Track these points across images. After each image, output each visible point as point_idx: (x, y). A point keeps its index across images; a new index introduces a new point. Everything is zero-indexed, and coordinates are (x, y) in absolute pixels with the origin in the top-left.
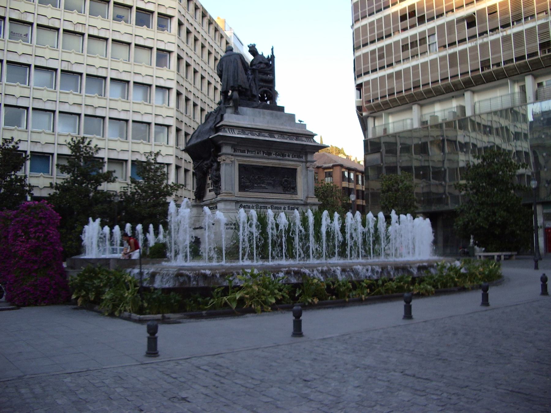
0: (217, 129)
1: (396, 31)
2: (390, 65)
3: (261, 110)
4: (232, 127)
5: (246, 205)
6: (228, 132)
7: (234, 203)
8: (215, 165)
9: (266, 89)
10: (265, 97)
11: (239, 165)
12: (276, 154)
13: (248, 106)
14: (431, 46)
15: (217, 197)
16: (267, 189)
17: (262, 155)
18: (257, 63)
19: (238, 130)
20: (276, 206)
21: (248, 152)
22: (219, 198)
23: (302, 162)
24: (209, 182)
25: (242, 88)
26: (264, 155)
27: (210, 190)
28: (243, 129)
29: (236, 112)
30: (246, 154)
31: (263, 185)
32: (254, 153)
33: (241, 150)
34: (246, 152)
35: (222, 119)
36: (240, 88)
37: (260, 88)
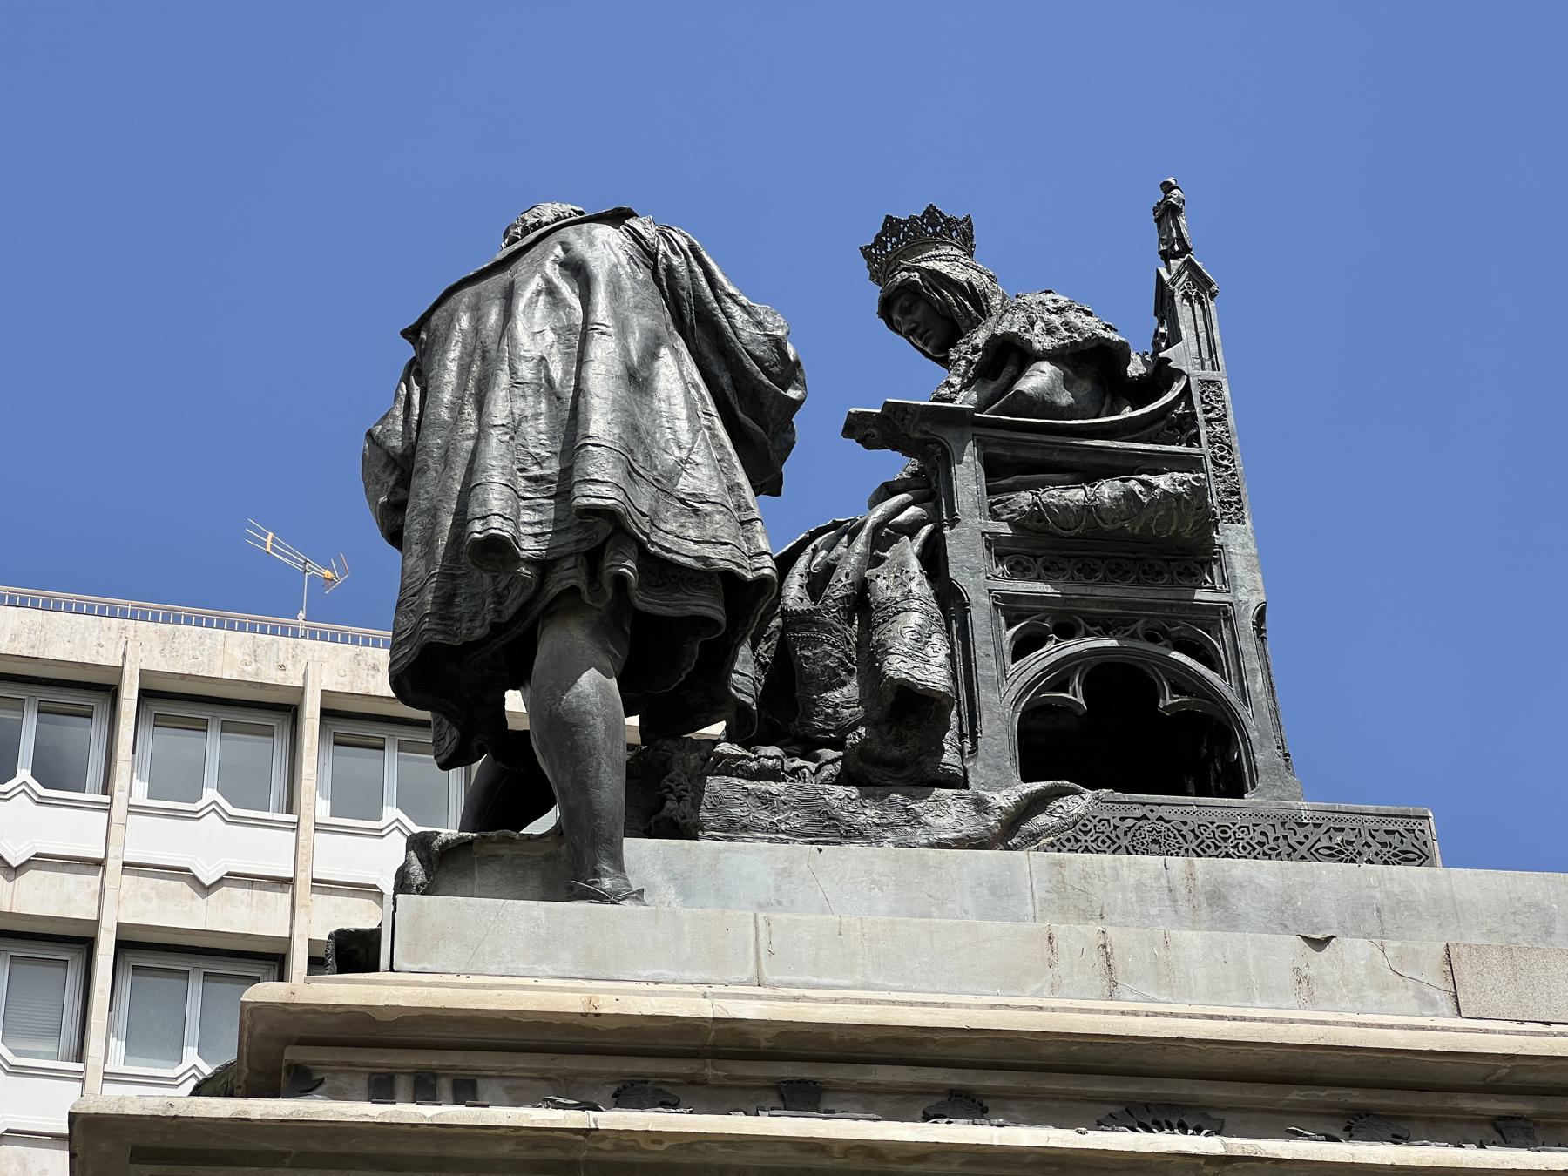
25: (661, 570)
37: (1023, 647)
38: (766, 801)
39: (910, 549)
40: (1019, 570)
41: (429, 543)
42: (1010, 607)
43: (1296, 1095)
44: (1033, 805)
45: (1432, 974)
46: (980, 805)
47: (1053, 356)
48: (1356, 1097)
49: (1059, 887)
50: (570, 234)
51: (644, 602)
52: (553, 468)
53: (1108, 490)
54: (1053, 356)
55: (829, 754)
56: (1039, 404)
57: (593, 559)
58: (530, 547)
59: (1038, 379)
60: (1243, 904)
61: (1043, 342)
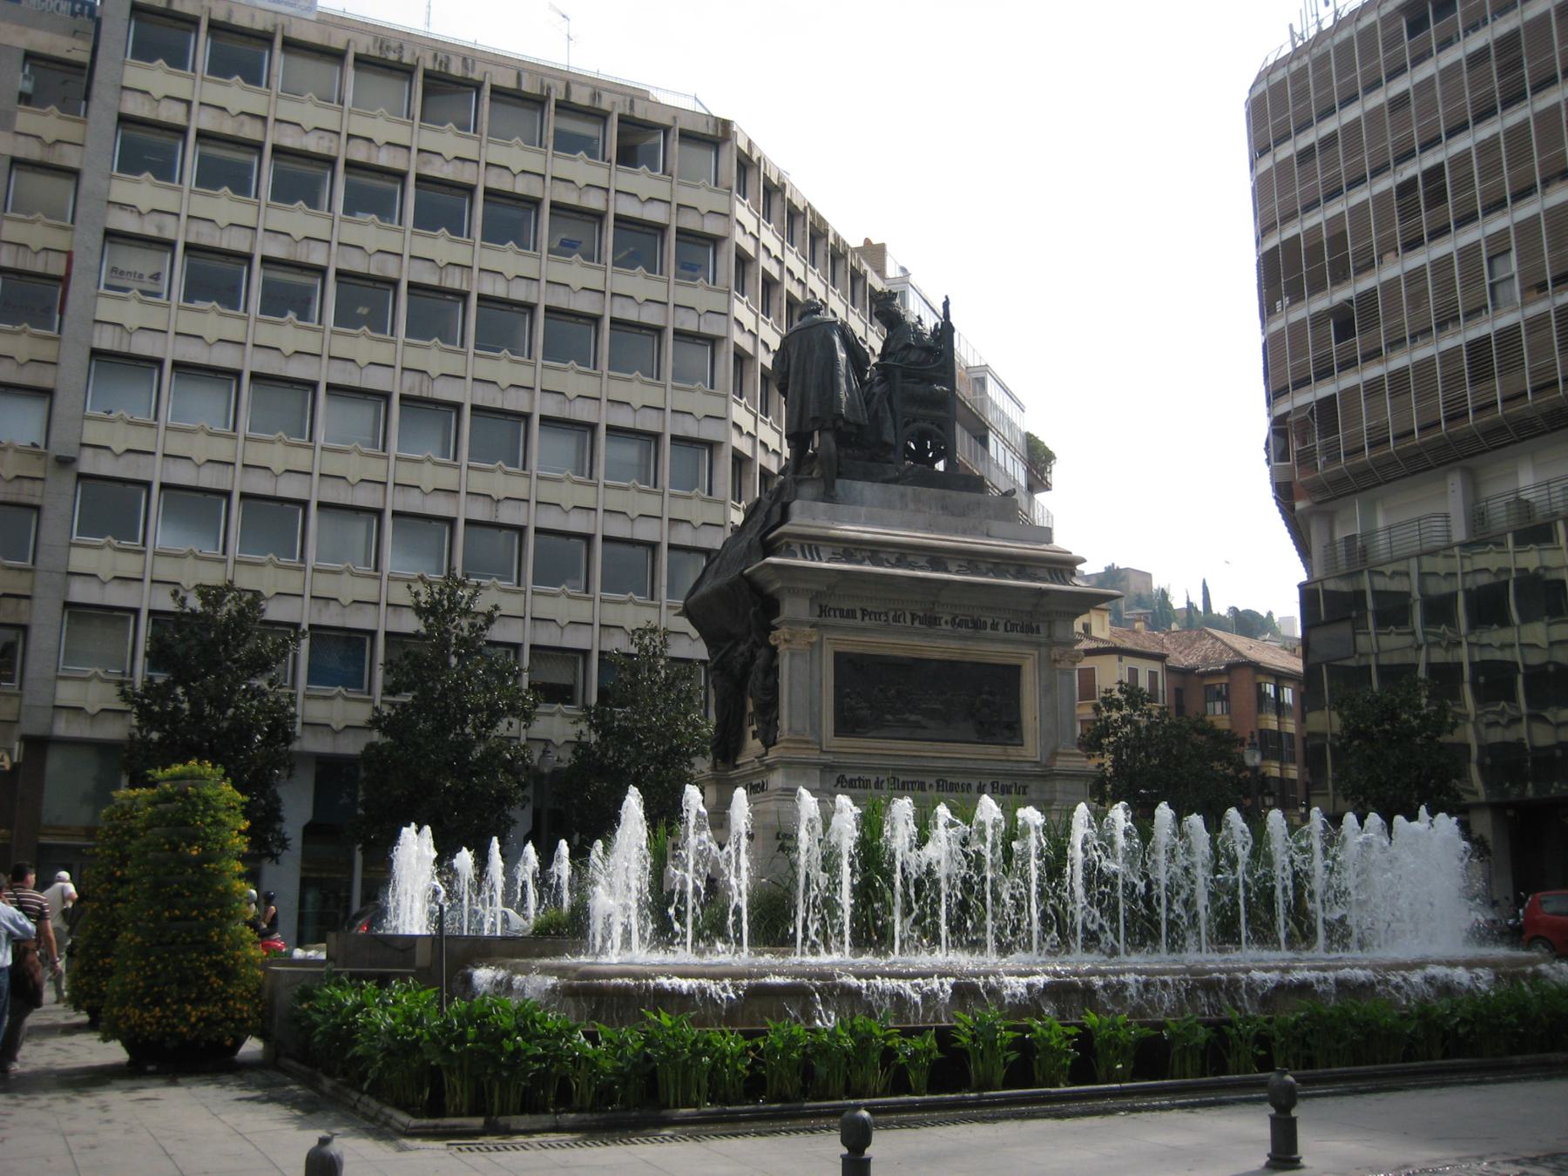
0: (769, 549)
1: (1387, 247)
2: (1373, 355)
3: (909, 490)
4: (813, 544)
5: (856, 776)
6: (799, 555)
7: (818, 772)
8: (762, 654)
9: (926, 425)
10: (929, 451)
11: (839, 657)
12: (954, 620)
13: (868, 476)
14: (1500, 291)
15: (766, 754)
16: (925, 728)
17: (909, 623)
18: (900, 346)
19: (830, 550)
20: (955, 781)
21: (863, 616)
22: (773, 754)
23: (1038, 645)
24: (750, 708)
26: (917, 624)
27: (754, 732)
28: (851, 548)
29: (829, 496)
30: (858, 622)
31: (913, 718)
32: (883, 618)
33: (841, 610)
34: (859, 614)
35: (785, 517)
36: (841, 423)
37: (906, 425)
46: (898, 470)
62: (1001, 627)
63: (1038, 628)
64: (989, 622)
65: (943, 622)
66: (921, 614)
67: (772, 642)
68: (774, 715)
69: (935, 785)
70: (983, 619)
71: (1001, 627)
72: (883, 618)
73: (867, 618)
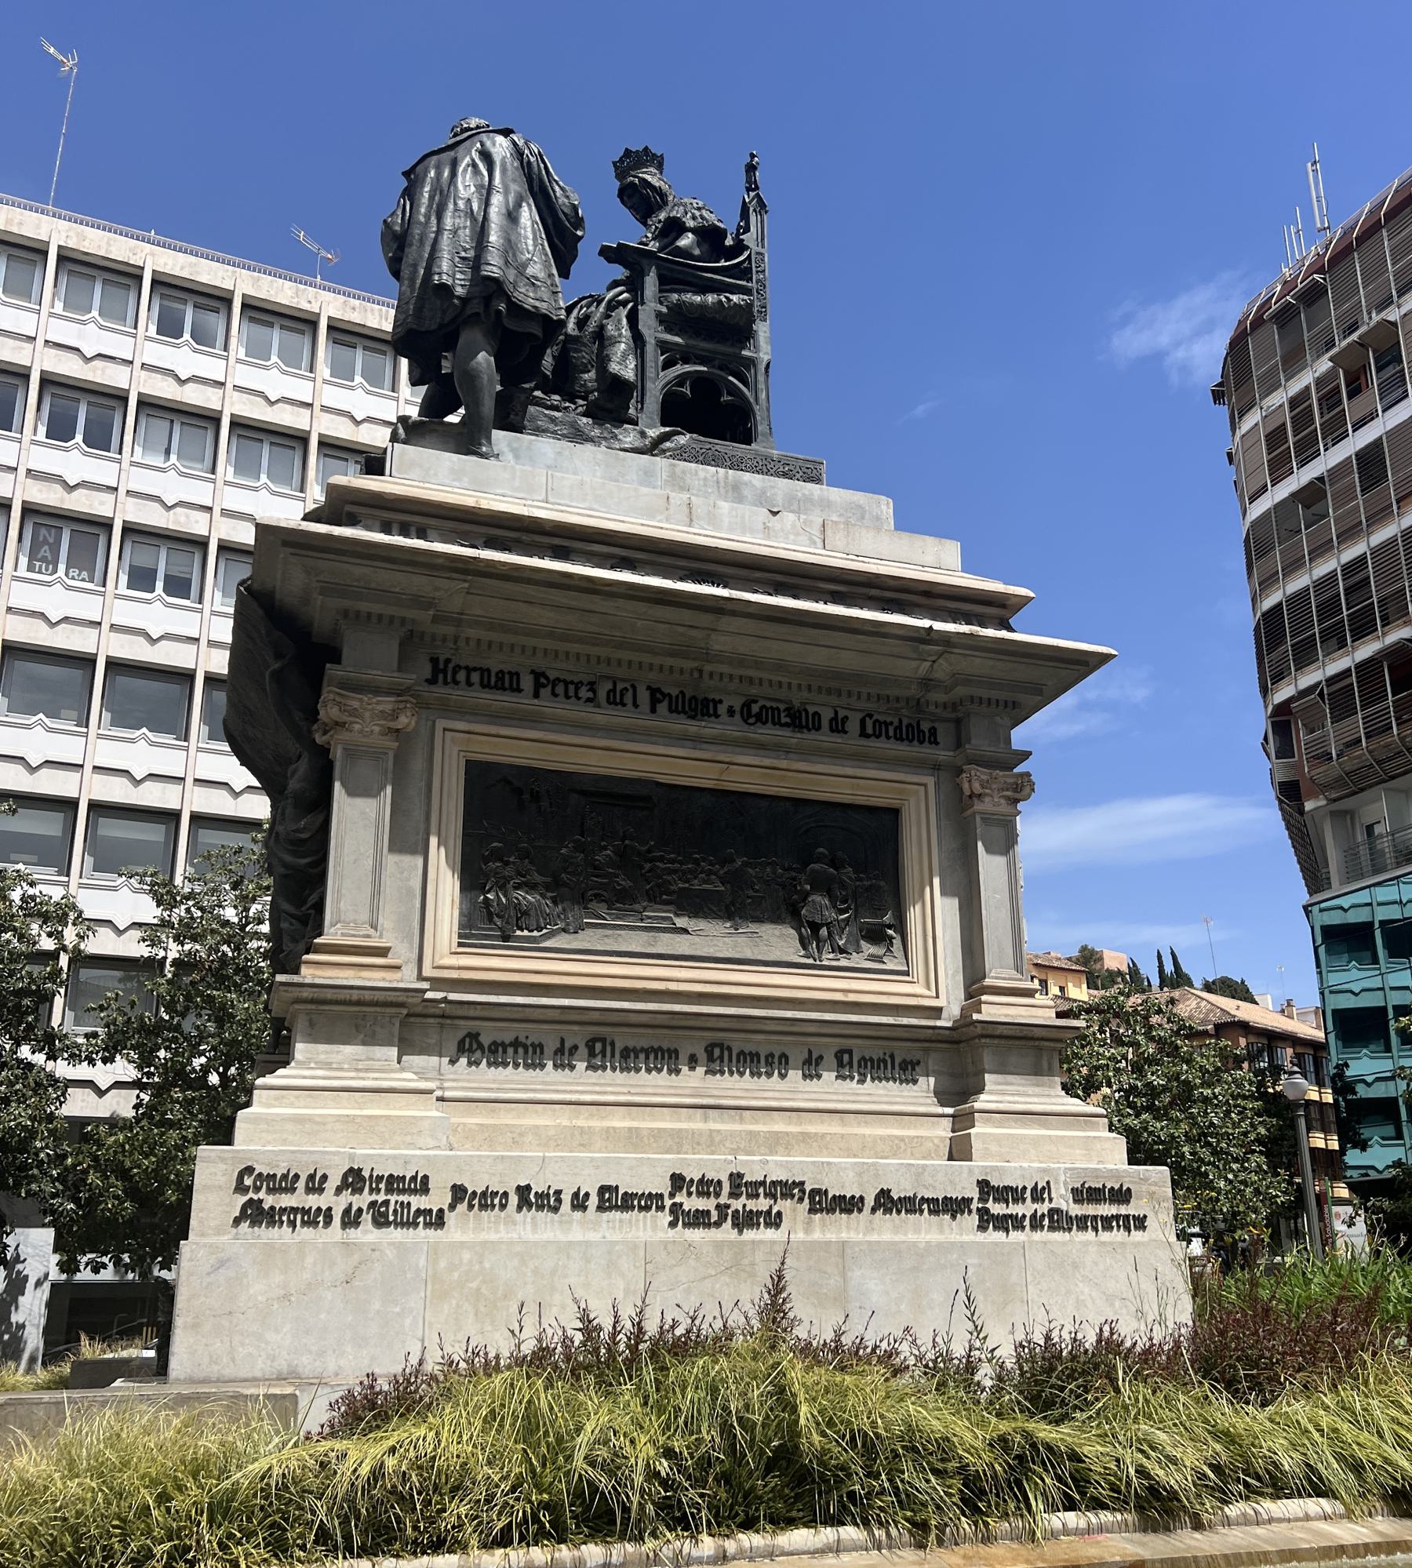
12: (747, 705)
23: (936, 768)
25: (516, 309)
30: (524, 702)
32: (584, 693)
33: (485, 672)
34: (527, 682)
37: (667, 365)
38: (553, 420)
39: (623, 313)
40: (669, 330)
41: (412, 280)
42: (663, 346)
43: (758, 575)
44: (665, 437)
45: (816, 531)
46: (643, 434)
47: (693, 230)
48: (779, 578)
49: (673, 475)
50: (484, 137)
51: (508, 323)
52: (471, 254)
53: (711, 298)
54: (693, 230)
55: (581, 402)
56: (684, 253)
57: (487, 300)
58: (459, 291)
59: (686, 241)
60: (746, 492)
61: (691, 224)
62: (853, 726)
63: (933, 732)
64: (827, 715)
65: (722, 709)
66: (674, 692)
67: (319, 739)
68: (313, 899)
69: (702, 1056)
70: (811, 709)
71: (853, 726)
72: (584, 693)
73: (545, 692)
